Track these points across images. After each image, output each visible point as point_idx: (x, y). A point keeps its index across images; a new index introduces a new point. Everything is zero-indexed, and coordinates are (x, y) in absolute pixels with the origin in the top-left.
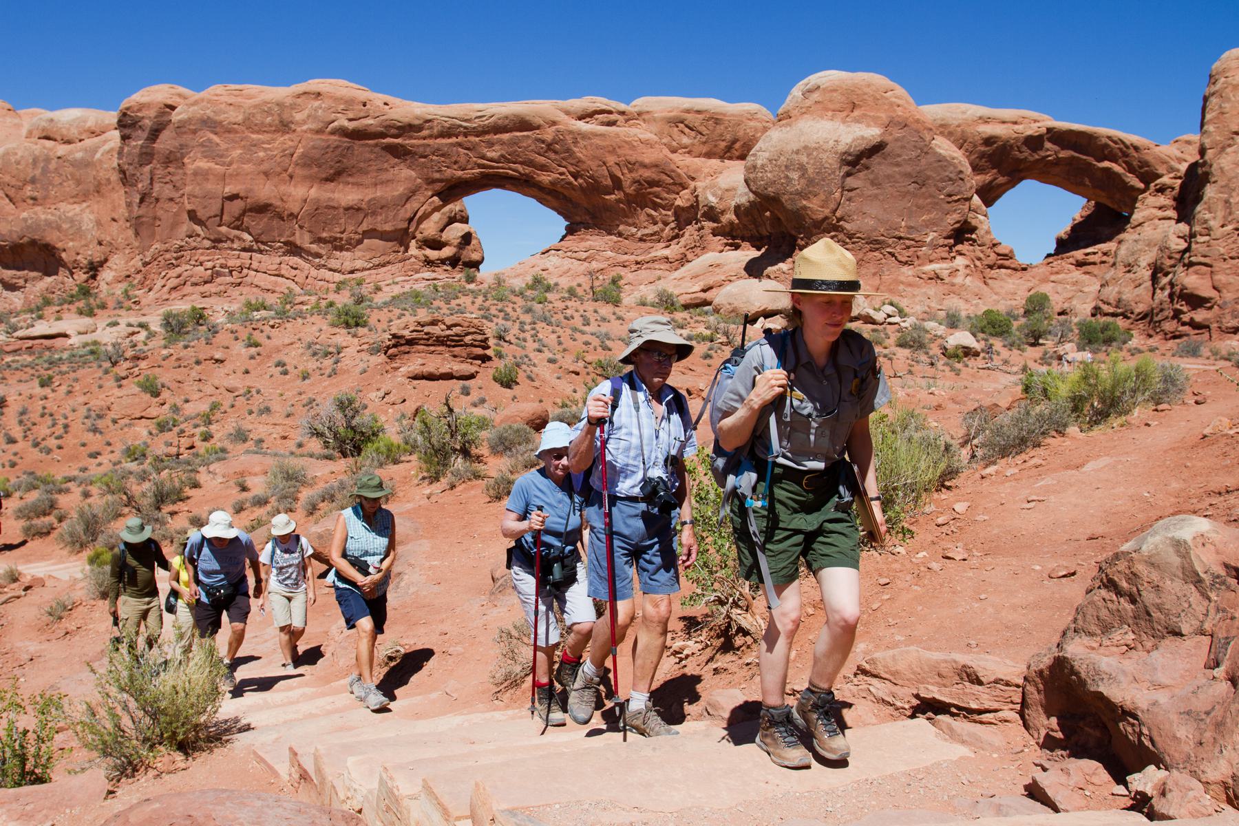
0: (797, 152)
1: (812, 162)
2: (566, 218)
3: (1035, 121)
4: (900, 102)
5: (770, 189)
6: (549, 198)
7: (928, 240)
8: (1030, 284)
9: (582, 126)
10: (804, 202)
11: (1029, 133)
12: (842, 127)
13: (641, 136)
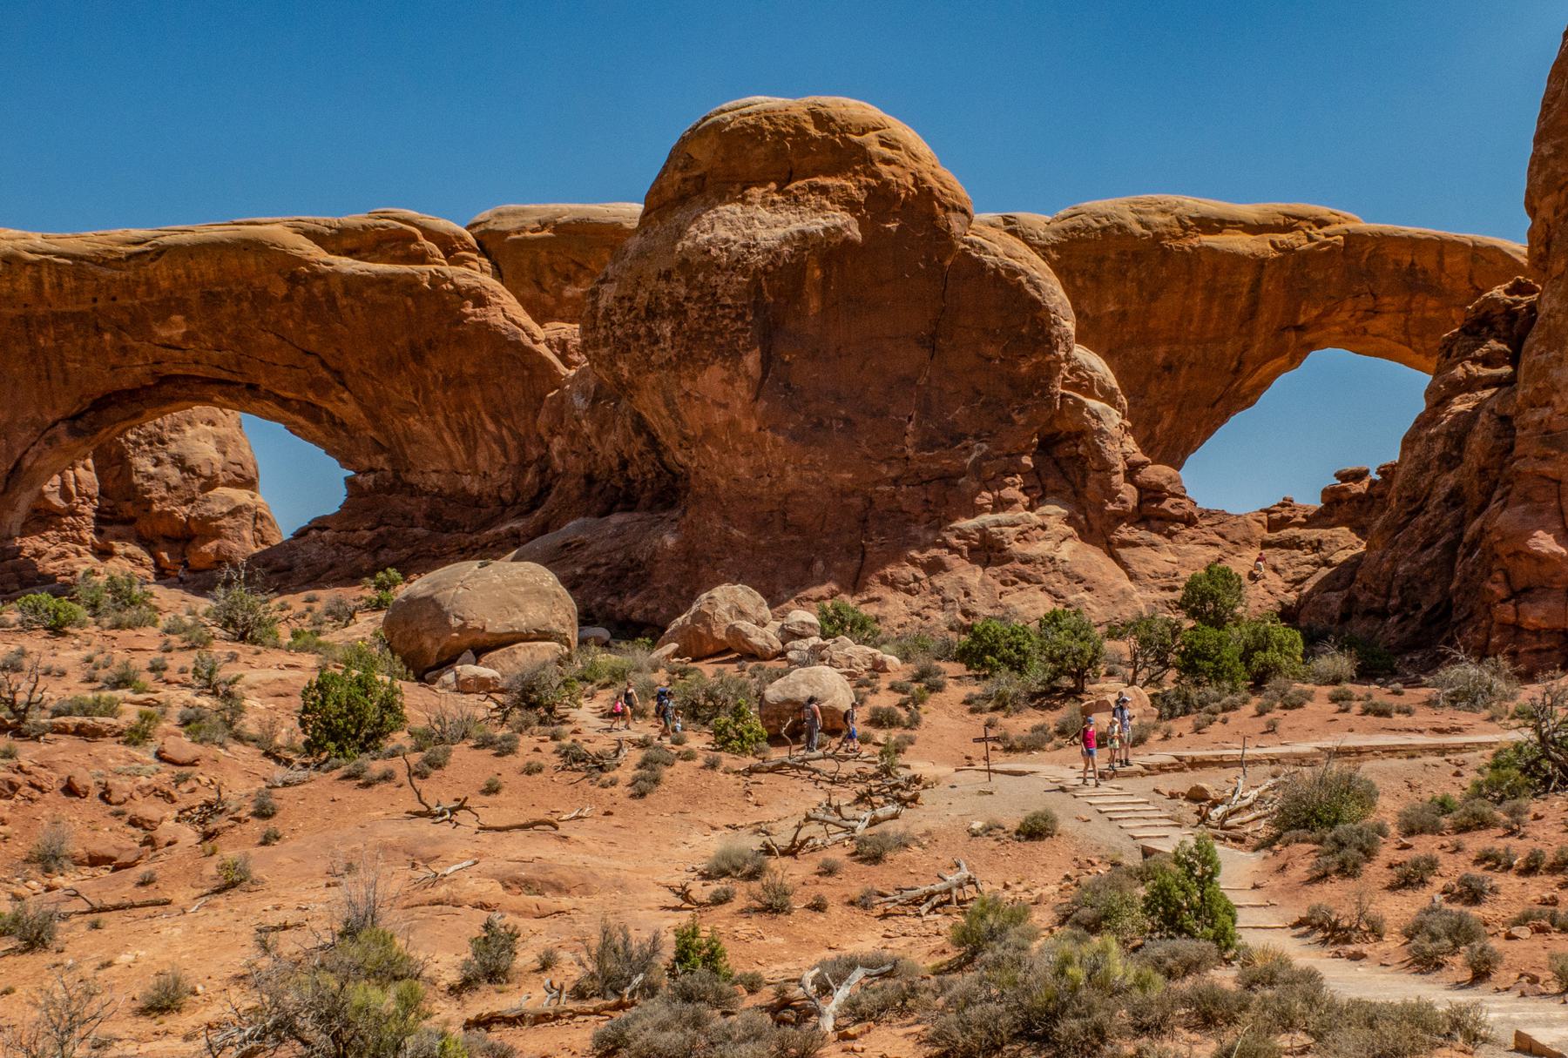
0: (667, 276)
1: (696, 294)
2: (346, 461)
3: (1321, 223)
4: (887, 152)
5: (620, 364)
6: (301, 420)
7: (968, 461)
8: (1214, 553)
9: (348, 265)
10: (687, 385)
11: (1306, 245)
12: (764, 213)
13: (462, 281)
